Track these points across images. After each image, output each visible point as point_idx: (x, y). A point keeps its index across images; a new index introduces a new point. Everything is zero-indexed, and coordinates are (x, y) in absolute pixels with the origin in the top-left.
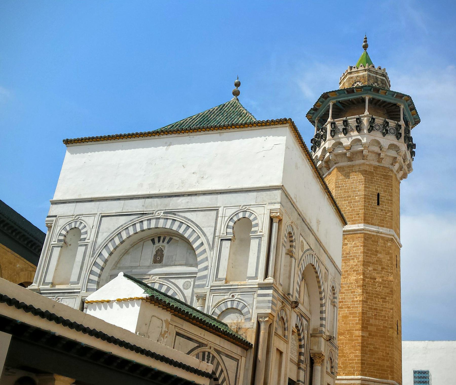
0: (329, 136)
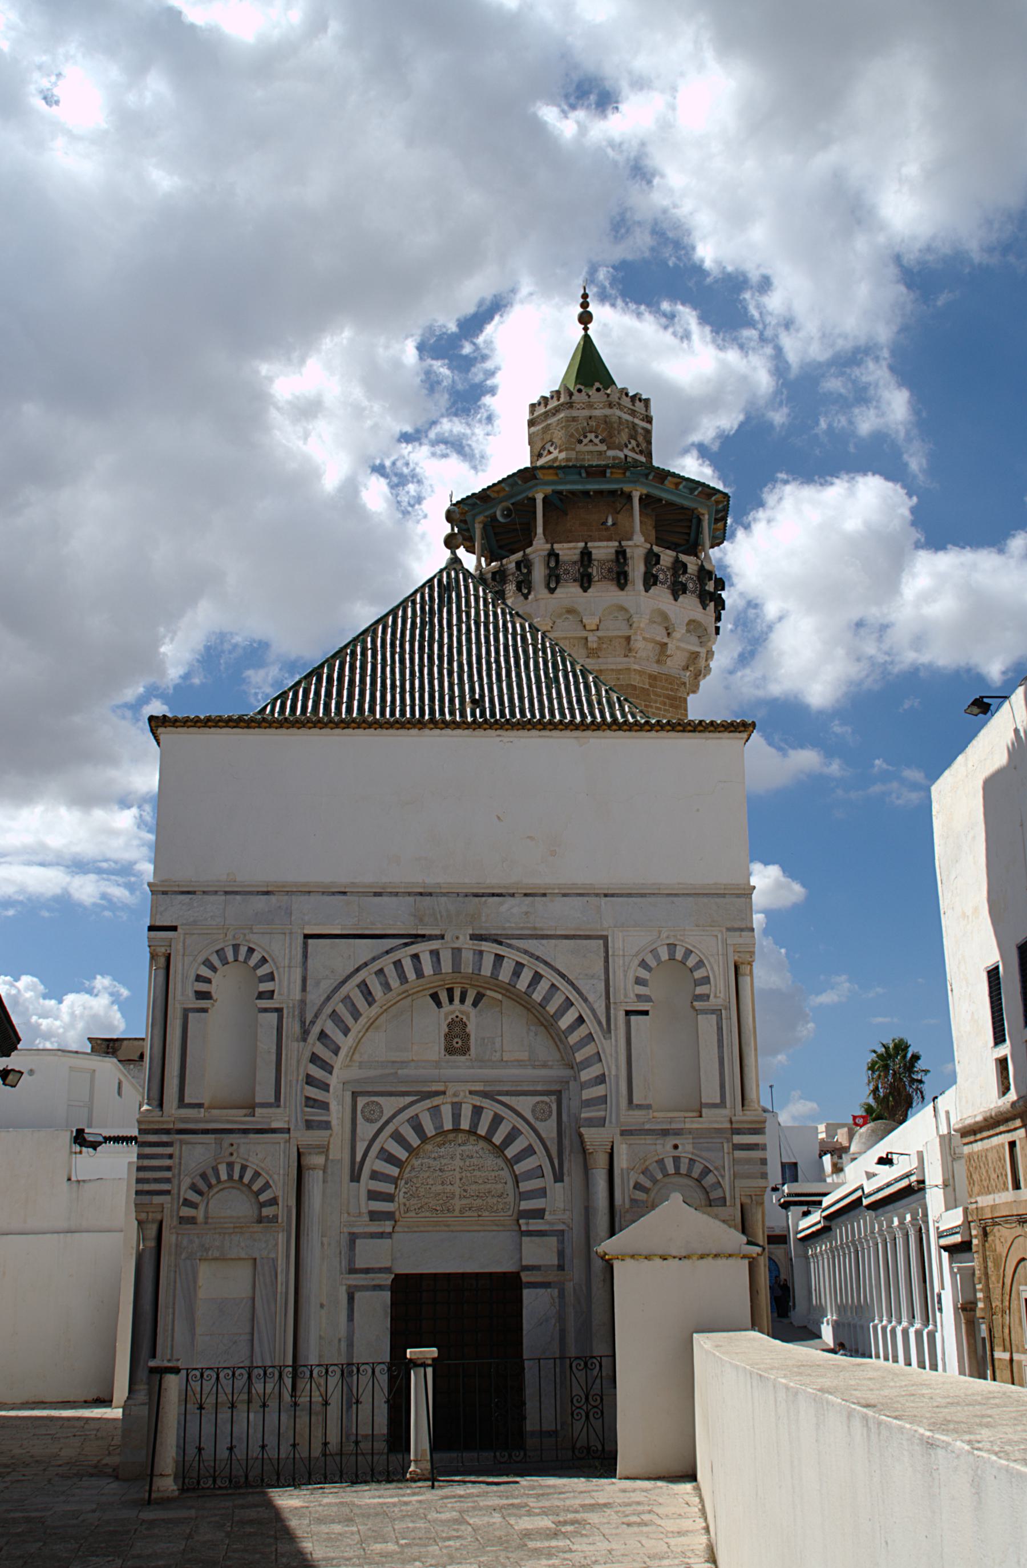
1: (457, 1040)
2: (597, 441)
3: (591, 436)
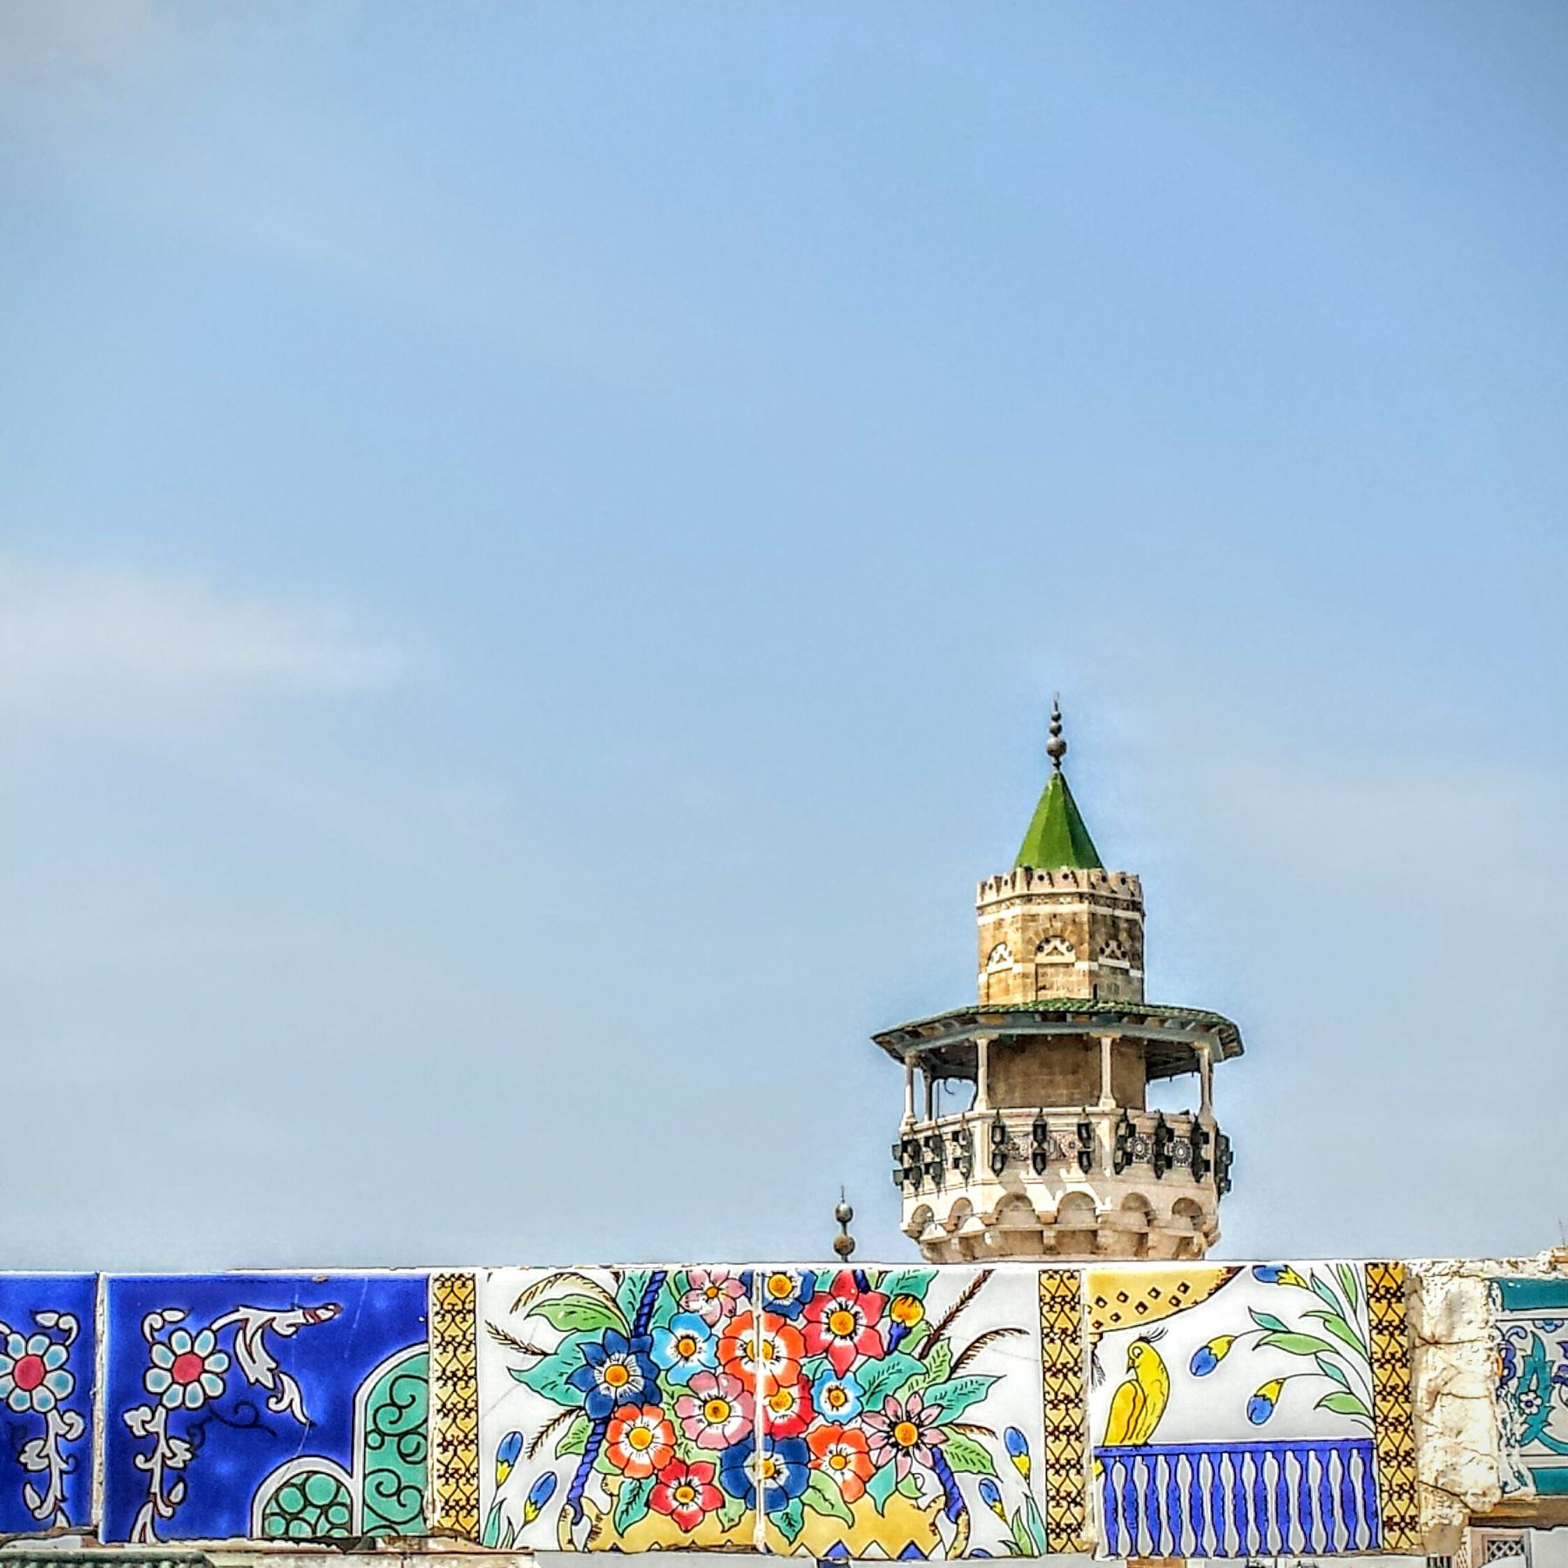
0: (981, 1170)
2: (1062, 948)
3: (1057, 943)
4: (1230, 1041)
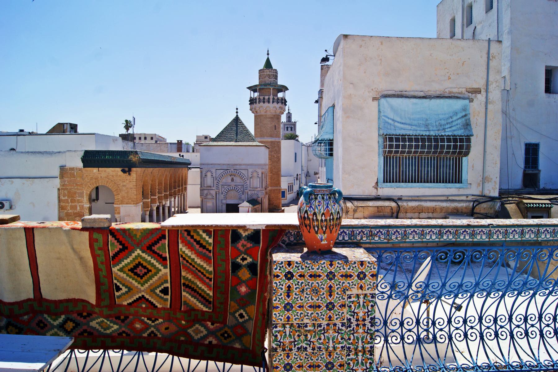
1: (232, 180)
4: (287, 89)
